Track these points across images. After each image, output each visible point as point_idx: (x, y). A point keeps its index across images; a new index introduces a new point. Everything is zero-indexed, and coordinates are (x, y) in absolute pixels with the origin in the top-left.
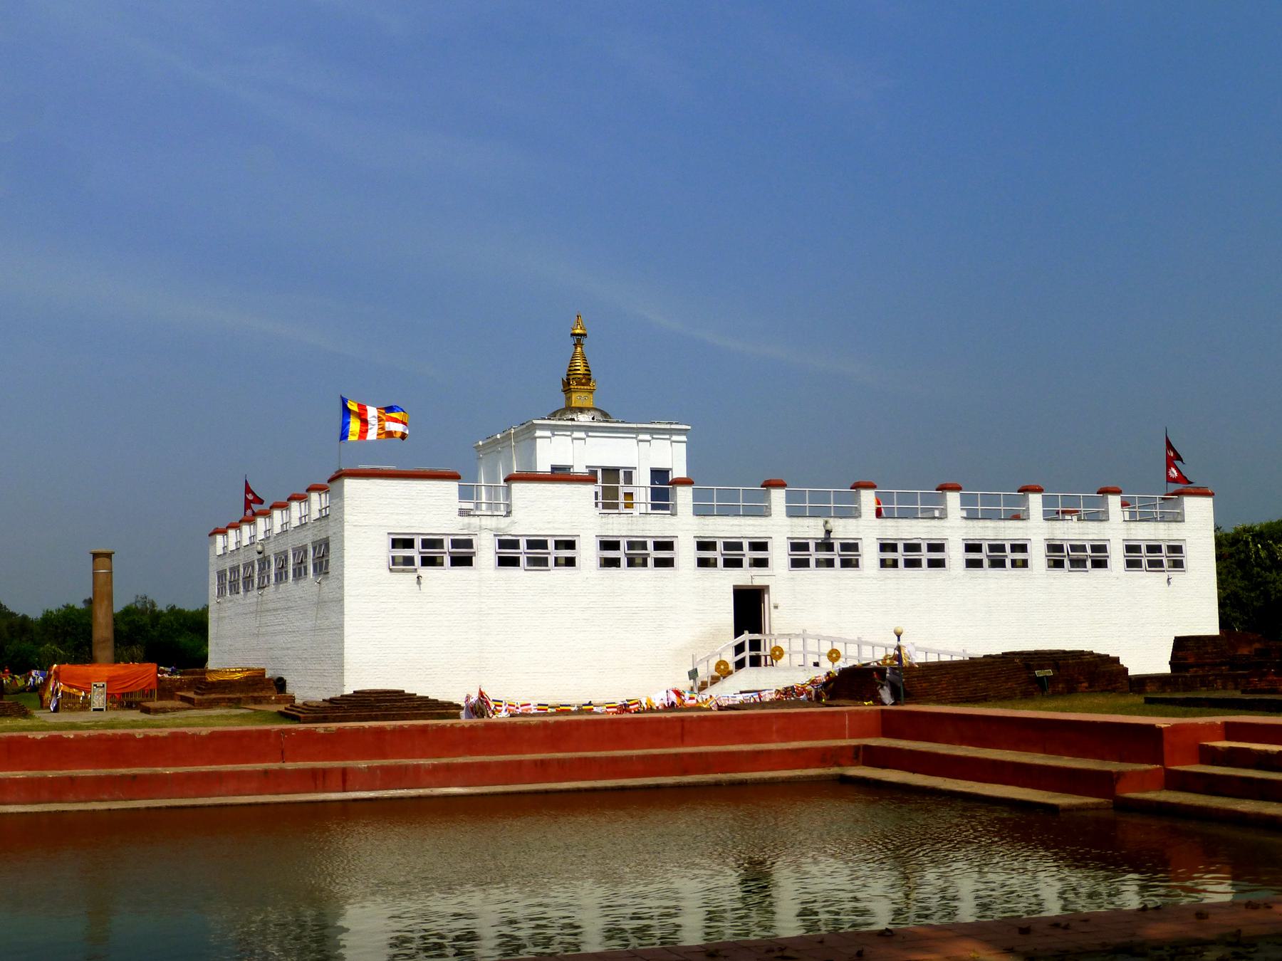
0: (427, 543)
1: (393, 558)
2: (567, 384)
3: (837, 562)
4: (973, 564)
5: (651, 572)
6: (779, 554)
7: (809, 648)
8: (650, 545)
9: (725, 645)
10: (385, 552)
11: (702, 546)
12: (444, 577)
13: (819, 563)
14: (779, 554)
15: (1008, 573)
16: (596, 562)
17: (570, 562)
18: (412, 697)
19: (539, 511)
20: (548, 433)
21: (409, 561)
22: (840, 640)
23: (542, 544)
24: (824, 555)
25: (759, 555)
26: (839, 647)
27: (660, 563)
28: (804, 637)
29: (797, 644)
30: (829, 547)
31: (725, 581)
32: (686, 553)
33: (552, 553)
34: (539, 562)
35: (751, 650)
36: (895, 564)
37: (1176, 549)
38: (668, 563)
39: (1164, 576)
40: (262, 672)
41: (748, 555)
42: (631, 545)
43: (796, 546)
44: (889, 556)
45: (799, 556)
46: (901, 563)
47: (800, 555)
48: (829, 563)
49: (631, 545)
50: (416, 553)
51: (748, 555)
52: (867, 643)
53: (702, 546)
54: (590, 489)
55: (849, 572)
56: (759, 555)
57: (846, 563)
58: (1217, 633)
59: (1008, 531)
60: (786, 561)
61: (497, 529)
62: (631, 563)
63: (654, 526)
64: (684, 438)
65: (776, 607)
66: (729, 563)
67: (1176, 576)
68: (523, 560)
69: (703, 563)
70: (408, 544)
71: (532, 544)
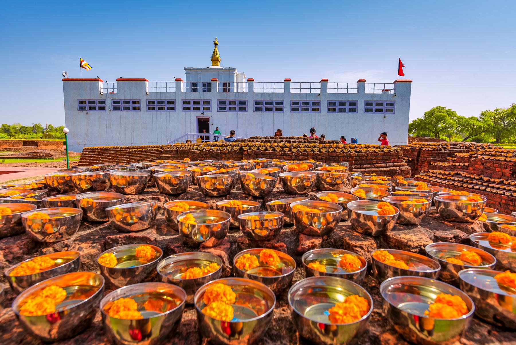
6: (214, 106)
10: (76, 105)
13: (230, 109)
14: (214, 106)
24: (232, 106)
30: (235, 103)
31: (193, 117)
35: (203, 139)
38: (173, 109)
43: (221, 103)
45: (223, 106)
47: (223, 106)
50: (87, 105)
51: (201, 106)
53: (185, 103)
57: (241, 109)
67: (389, 115)
68: (122, 108)
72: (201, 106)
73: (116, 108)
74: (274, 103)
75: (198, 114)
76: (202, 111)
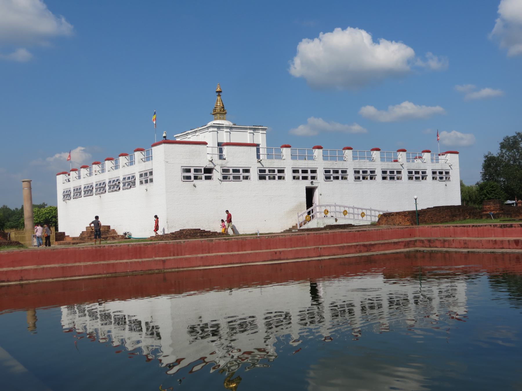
0: (196, 171)
1: (184, 177)
2: (215, 110)
3: (340, 178)
4: (384, 178)
5: (277, 181)
6: (320, 175)
7: (334, 210)
8: (276, 171)
9: (304, 210)
10: (179, 174)
11: (295, 171)
12: (202, 183)
14: (320, 175)
15: (396, 181)
16: (257, 177)
17: (246, 178)
18: (204, 231)
19: (236, 158)
20: (216, 129)
21: (189, 178)
22: (346, 207)
23: (238, 171)
25: (313, 175)
26: (347, 209)
27: (280, 178)
28: (335, 206)
29: (332, 209)
32: (288, 174)
33: (242, 174)
34: (237, 178)
36: (359, 178)
37: (447, 173)
39: (444, 183)
40: (109, 227)
41: (309, 175)
42: (270, 171)
44: (357, 175)
46: (361, 178)
48: (337, 178)
49: (270, 171)
50: (192, 174)
52: (356, 208)
53: (295, 171)
54: (255, 149)
55: (344, 181)
56: (313, 175)
57: (342, 178)
58: (460, 204)
59: (395, 166)
60: (323, 177)
61: (222, 165)
62: (270, 178)
63: (276, 164)
64: (265, 132)
65: (321, 195)
66: (305, 178)
67: (448, 183)
69: (294, 178)
70: (188, 171)
71: (235, 171)
72: (309, 175)
73: (225, 178)
74: (369, 172)
75: (307, 183)
76: (310, 180)
